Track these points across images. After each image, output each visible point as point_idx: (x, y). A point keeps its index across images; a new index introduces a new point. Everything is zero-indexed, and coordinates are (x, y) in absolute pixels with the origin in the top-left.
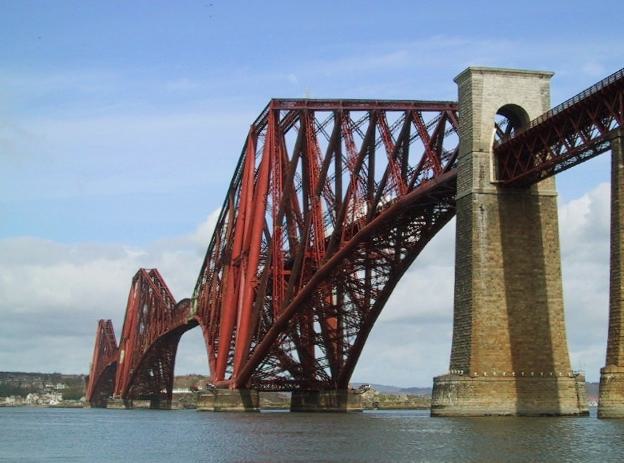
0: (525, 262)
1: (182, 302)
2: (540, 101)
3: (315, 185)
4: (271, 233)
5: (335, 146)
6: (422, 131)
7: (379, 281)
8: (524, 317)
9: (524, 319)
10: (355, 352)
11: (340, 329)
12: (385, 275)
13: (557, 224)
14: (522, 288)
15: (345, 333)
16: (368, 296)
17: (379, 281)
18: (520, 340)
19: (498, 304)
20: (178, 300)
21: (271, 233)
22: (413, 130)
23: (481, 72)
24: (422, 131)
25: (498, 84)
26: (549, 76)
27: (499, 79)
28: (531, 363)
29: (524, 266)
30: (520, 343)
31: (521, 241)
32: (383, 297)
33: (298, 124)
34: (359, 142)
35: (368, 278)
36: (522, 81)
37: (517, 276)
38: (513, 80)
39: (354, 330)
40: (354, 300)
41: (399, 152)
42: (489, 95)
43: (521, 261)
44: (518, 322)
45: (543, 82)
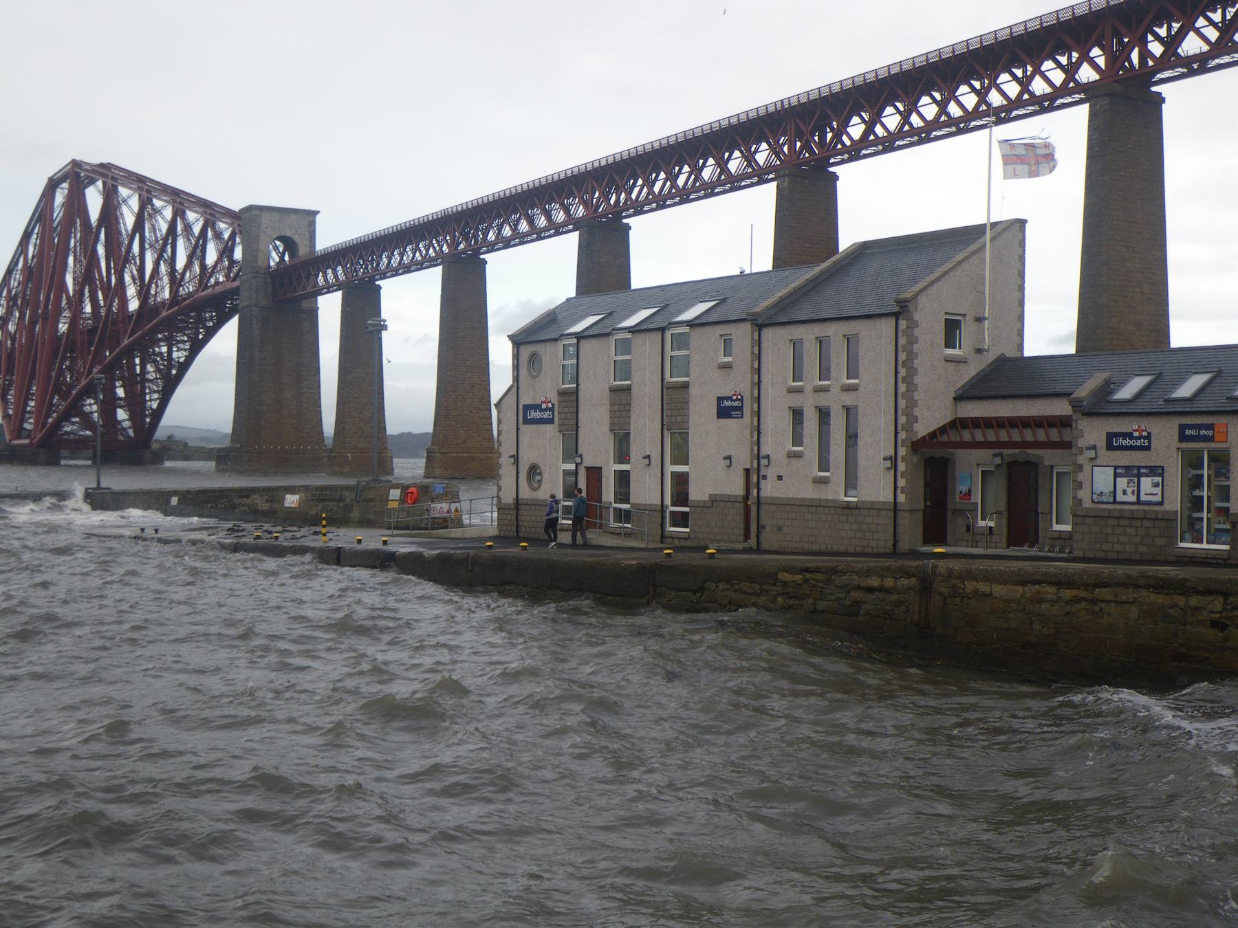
2: (307, 233)
3: (120, 257)
4: (71, 293)
5: (139, 226)
6: (218, 235)
7: (179, 355)
12: (185, 350)
15: (148, 397)
16: (170, 367)
17: (179, 355)
21: (71, 293)
22: (210, 234)
26: (316, 213)
32: (184, 367)
34: (164, 227)
35: (170, 352)
36: (293, 217)
39: (156, 396)
40: (158, 370)
41: (197, 252)
45: (311, 218)
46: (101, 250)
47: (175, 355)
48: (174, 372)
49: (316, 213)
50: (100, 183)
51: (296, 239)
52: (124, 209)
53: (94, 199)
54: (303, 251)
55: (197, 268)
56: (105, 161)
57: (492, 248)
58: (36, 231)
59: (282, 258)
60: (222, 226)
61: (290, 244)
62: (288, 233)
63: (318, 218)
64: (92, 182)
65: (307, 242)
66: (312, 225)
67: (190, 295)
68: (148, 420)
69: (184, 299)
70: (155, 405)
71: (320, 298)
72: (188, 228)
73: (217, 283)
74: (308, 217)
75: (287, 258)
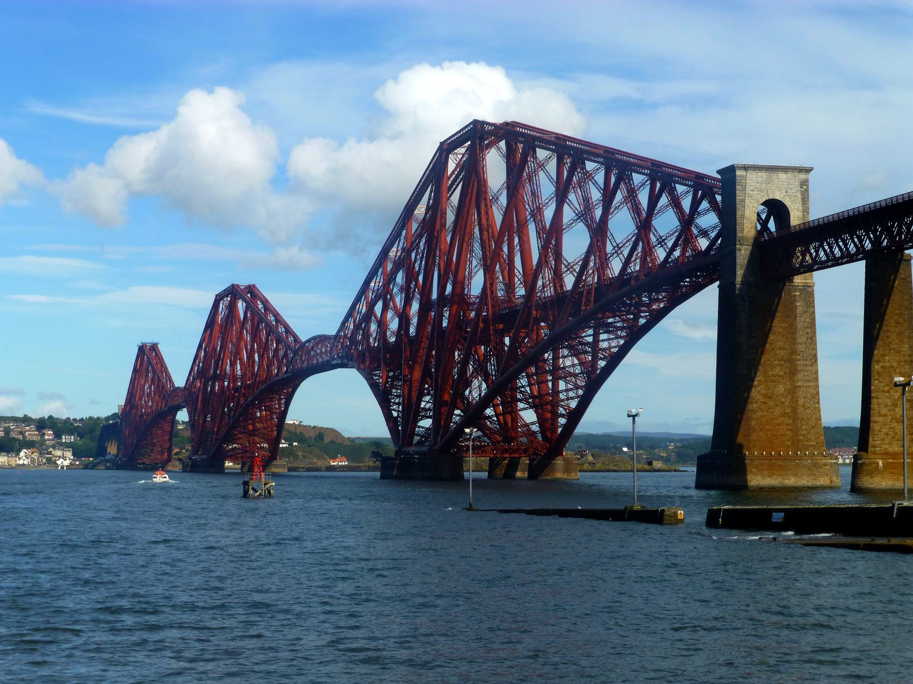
0: (784, 349)
1: (309, 341)
2: (799, 196)
6: (676, 203)
8: (784, 400)
9: (782, 403)
10: (575, 416)
11: (556, 392)
13: (814, 312)
14: (781, 373)
15: (562, 396)
18: (778, 422)
19: (759, 388)
20: (303, 338)
23: (745, 168)
24: (676, 203)
25: (760, 179)
26: (808, 170)
27: (763, 175)
28: (789, 443)
29: (782, 353)
30: (779, 425)
31: (781, 330)
32: (615, 360)
35: (596, 341)
36: (782, 176)
37: (776, 362)
38: (774, 176)
42: (752, 191)
43: (782, 348)
44: (777, 406)
45: (803, 176)
48: (602, 364)
50: (502, 144)
51: (787, 202)
54: (796, 219)
56: (509, 120)
59: (764, 223)
60: (680, 189)
62: (777, 197)
63: (811, 176)
66: (804, 183)
68: (562, 421)
70: (573, 404)
72: (632, 194)
75: (772, 225)
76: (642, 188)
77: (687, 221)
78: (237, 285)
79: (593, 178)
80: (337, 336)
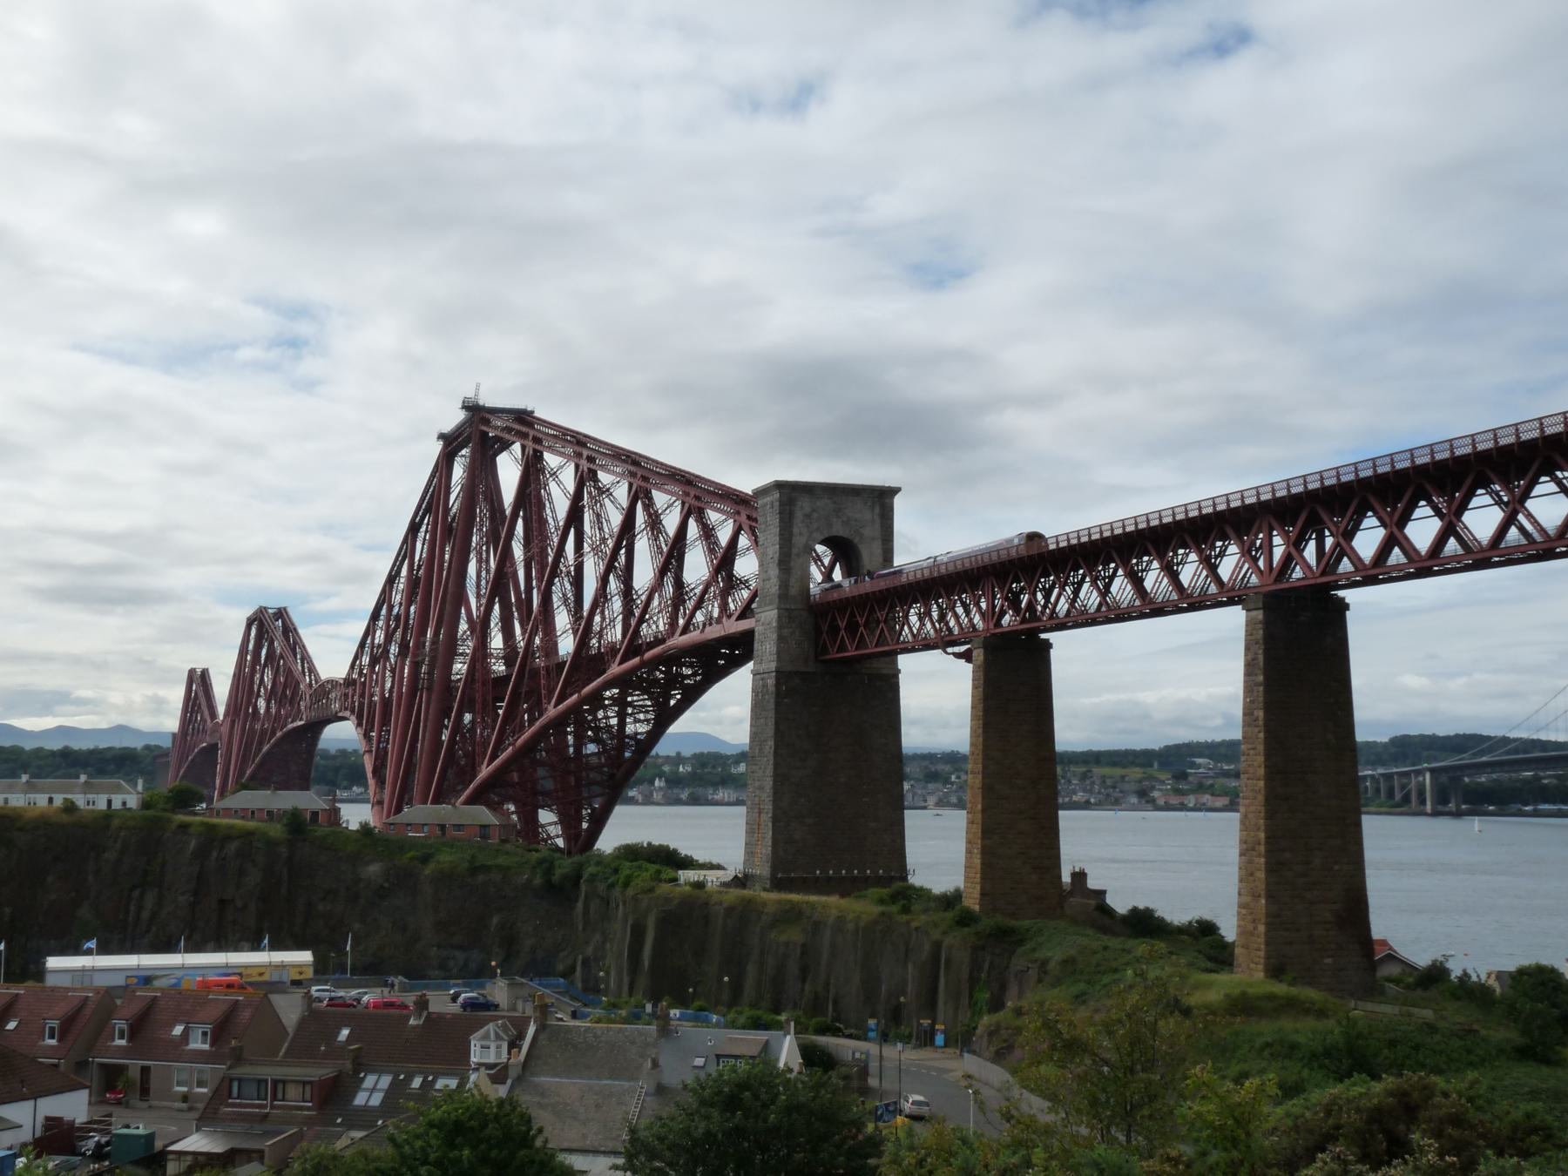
3: (546, 567)
5: (575, 516)
6: (708, 533)
12: (648, 721)
24: (708, 533)
26: (892, 492)
33: (517, 447)
34: (616, 519)
35: (622, 724)
41: (672, 560)
46: (518, 551)
47: (630, 729)
49: (892, 492)
52: (553, 486)
53: (509, 470)
55: (669, 589)
57: (1375, 573)
58: (426, 521)
59: (828, 576)
60: (713, 516)
61: (845, 551)
63: (898, 501)
64: (506, 446)
65: (877, 548)
67: (658, 641)
69: (651, 646)
71: (899, 656)
73: (709, 621)
74: (881, 499)
75: (837, 575)
76: (668, 511)
77: (724, 562)
78: (265, 608)
79: (611, 494)
80: (349, 682)
